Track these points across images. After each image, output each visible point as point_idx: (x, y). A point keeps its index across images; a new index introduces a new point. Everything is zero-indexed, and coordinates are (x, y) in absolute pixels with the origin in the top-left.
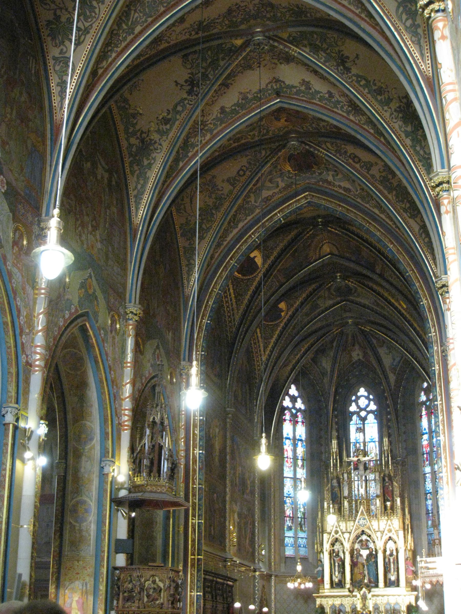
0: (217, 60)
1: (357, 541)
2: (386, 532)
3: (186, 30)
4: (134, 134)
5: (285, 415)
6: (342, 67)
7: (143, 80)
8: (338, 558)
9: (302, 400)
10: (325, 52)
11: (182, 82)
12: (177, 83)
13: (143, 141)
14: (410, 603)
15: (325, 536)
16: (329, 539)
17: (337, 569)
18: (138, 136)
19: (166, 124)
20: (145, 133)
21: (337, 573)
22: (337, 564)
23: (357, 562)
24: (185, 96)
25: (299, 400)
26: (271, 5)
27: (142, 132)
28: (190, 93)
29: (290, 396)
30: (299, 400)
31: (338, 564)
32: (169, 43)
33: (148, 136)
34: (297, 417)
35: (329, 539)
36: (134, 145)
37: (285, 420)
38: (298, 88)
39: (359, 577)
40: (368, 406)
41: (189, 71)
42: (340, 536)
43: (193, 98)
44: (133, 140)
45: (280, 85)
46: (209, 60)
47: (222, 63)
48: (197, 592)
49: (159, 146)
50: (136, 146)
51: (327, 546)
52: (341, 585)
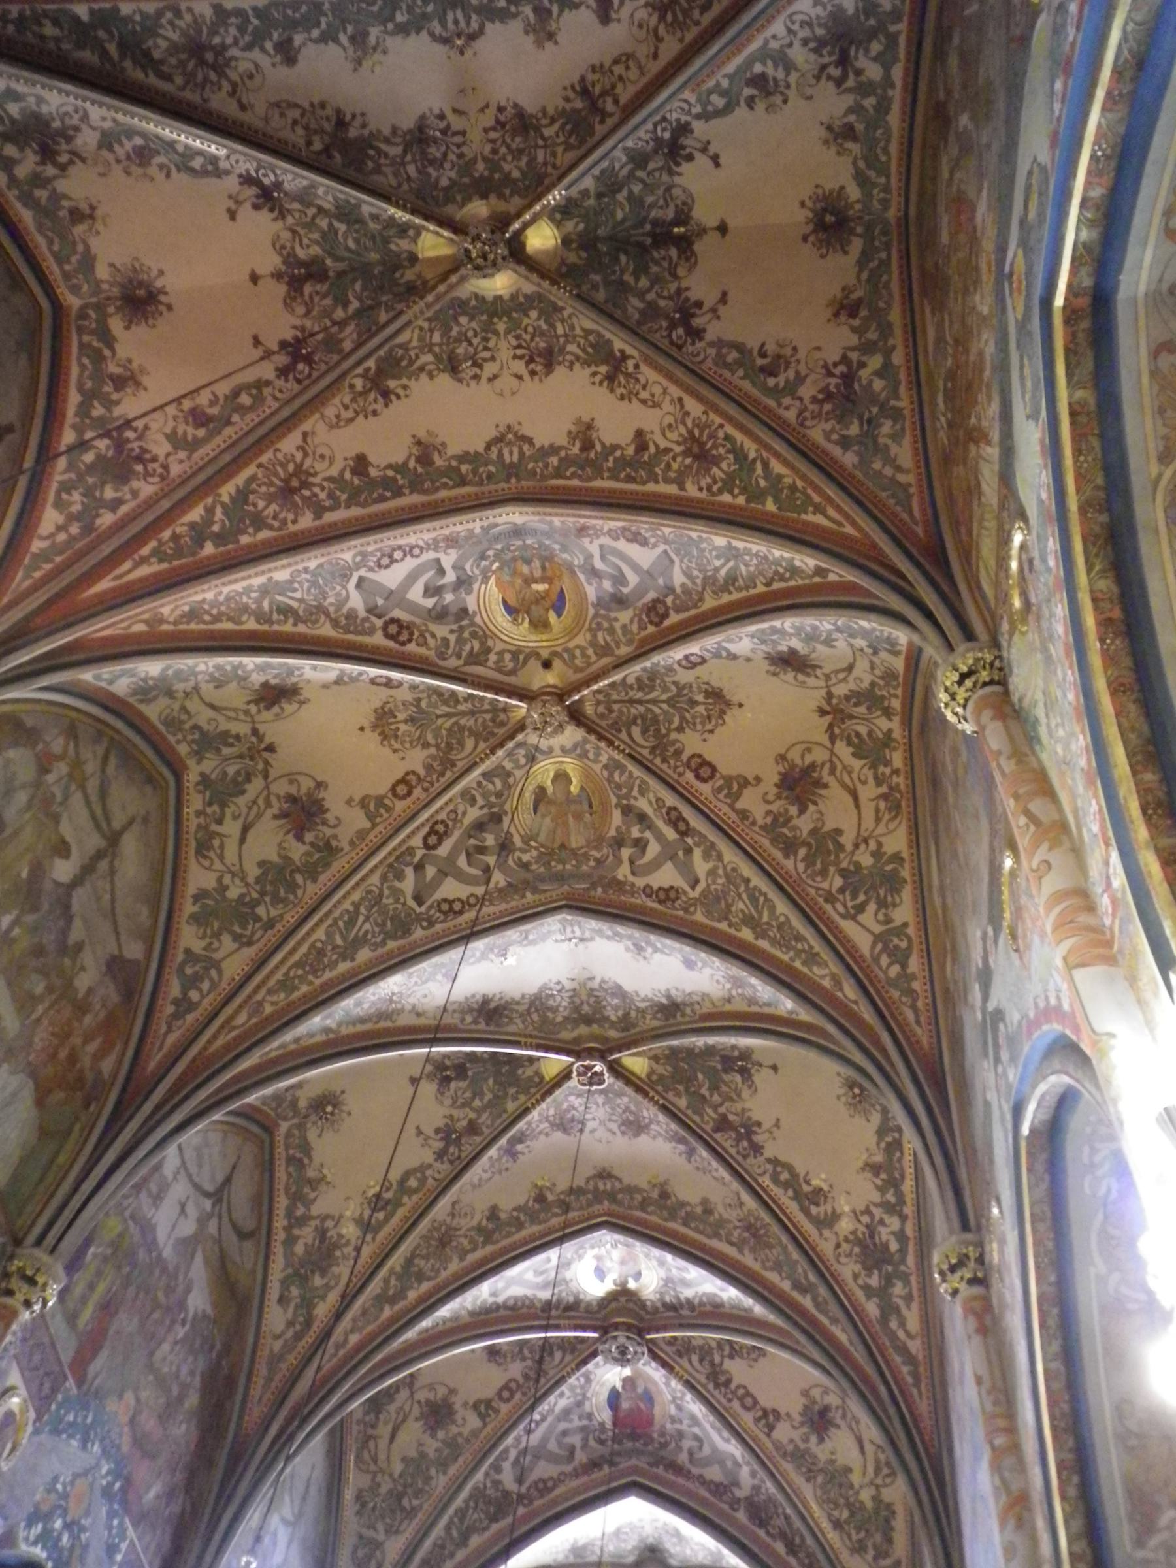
0: (600, 196)
3: (644, 395)
4: (865, 89)
6: (266, 181)
7: (803, 204)
10: (320, 210)
11: (702, 160)
12: (716, 160)
13: (844, 61)
18: (851, 76)
19: (763, 76)
20: (829, 78)
24: (698, 126)
26: (453, 367)
27: (839, 82)
28: (683, 129)
32: (680, 400)
33: (824, 67)
36: (875, 59)
38: (390, 26)
41: (677, 179)
43: (675, 116)
44: (874, 72)
45: (443, 24)
46: (622, 196)
47: (588, 183)
49: (796, 27)
50: (867, 50)
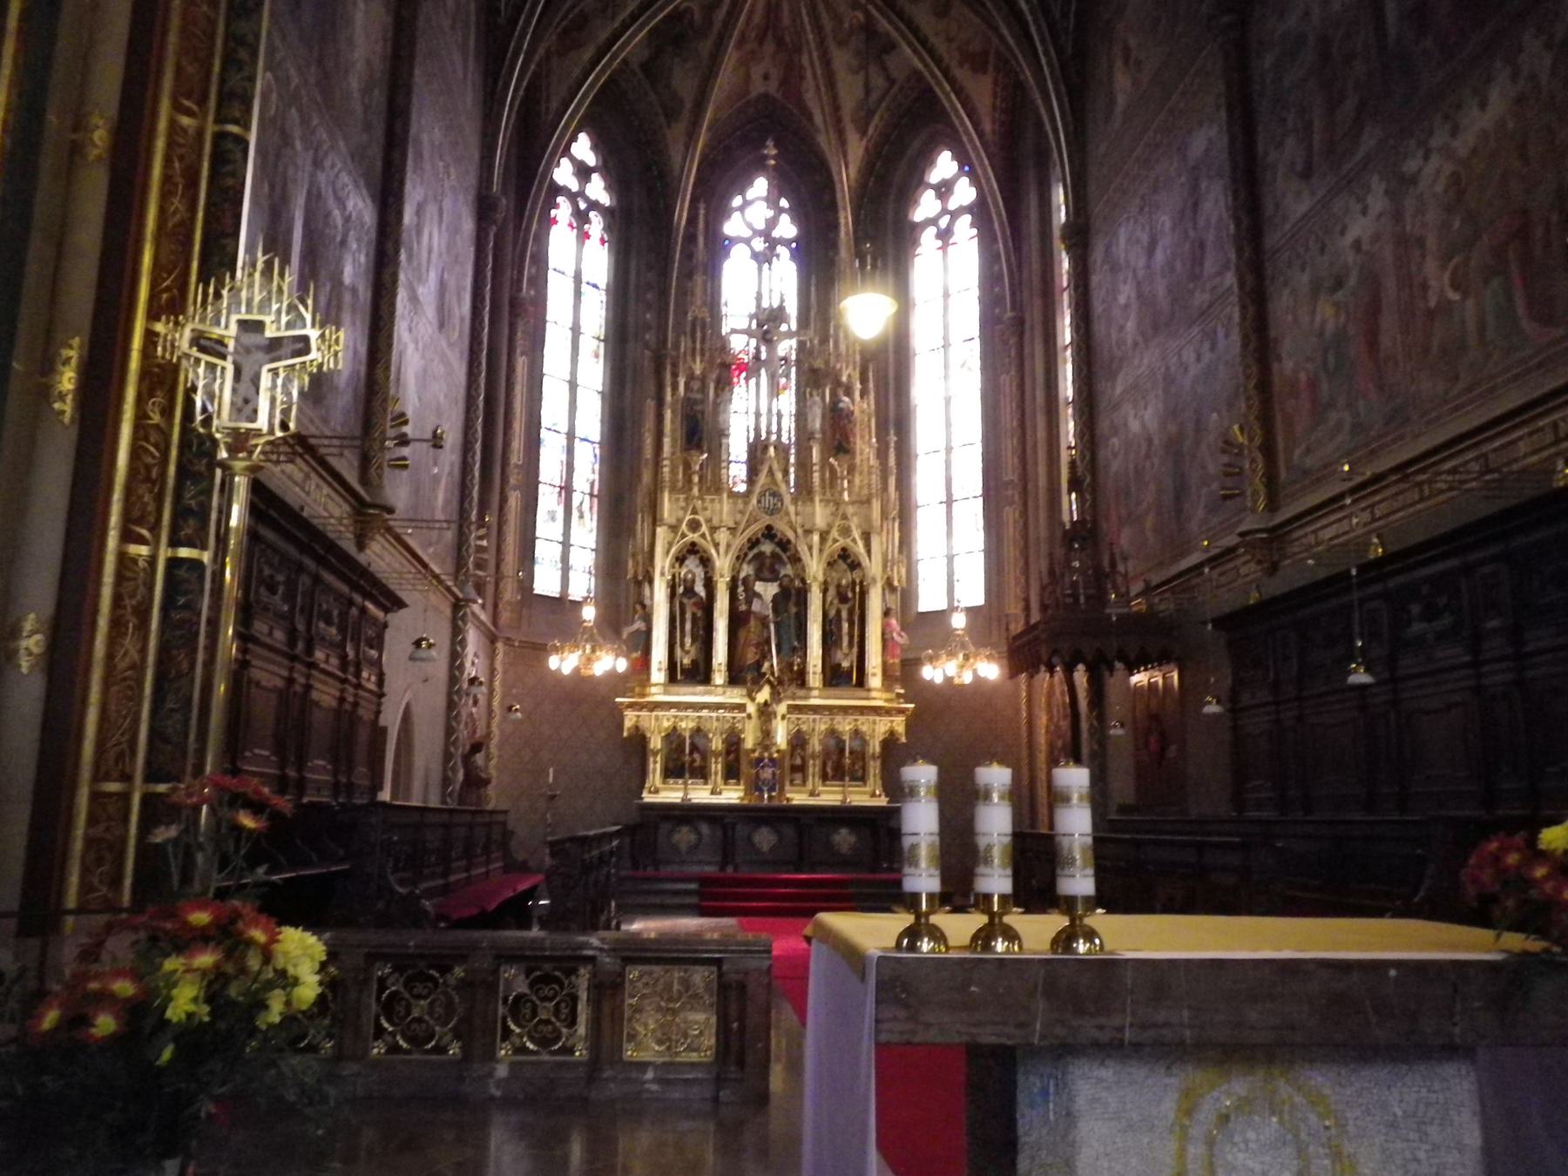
1: (751, 555)
2: (835, 533)
5: (556, 206)
8: (693, 600)
9: (604, 177)
14: (892, 733)
15: (661, 532)
16: (670, 544)
17: (688, 626)
21: (688, 640)
22: (688, 616)
23: (749, 612)
25: (596, 179)
29: (573, 159)
30: (595, 177)
31: (694, 615)
34: (588, 221)
35: (670, 544)
37: (555, 221)
39: (751, 656)
40: (772, 223)
42: (703, 536)
48: (174, 543)
51: (662, 563)
52: (699, 673)
